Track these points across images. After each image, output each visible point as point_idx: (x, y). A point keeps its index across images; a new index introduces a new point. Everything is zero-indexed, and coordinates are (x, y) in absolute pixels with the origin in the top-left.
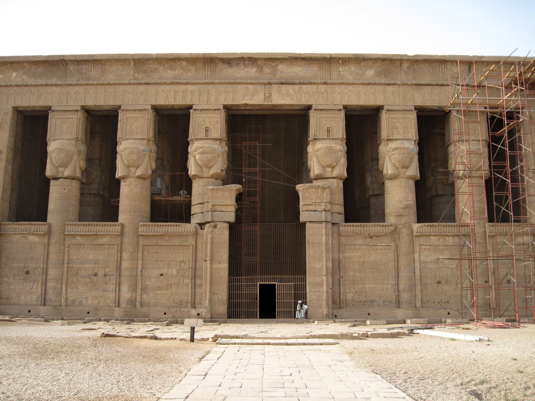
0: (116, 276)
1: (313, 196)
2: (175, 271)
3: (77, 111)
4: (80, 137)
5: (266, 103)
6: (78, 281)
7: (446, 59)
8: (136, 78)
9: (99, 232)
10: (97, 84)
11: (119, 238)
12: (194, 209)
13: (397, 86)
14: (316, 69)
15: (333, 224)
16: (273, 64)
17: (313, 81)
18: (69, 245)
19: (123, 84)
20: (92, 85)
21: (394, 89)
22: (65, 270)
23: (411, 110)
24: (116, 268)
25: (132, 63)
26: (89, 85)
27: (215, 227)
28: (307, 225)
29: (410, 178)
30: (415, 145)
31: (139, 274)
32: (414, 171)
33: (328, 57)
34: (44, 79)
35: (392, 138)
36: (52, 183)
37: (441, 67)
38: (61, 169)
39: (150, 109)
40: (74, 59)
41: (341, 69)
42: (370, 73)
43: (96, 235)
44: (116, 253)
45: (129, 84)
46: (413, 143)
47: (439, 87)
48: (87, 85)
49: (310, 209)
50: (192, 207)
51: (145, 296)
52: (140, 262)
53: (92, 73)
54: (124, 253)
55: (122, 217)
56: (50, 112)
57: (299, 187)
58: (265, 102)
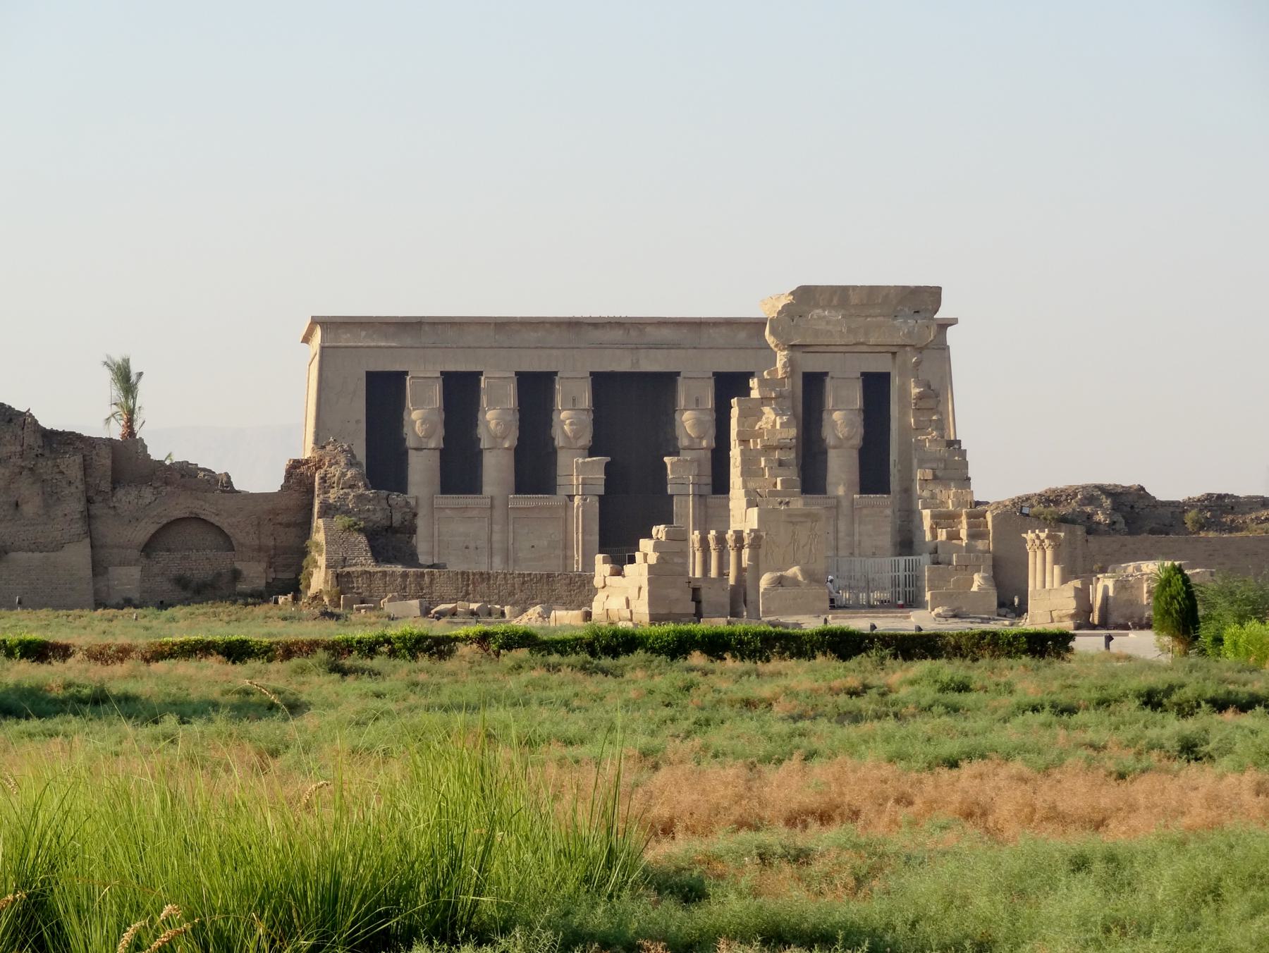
2: (546, 543)
3: (437, 378)
10: (457, 348)
11: (489, 511)
12: (560, 480)
14: (685, 331)
15: (700, 496)
16: (640, 326)
17: (682, 346)
22: (436, 544)
25: (493, 325)
27: (586, 500)
28: (675, 499)
31: (511, 547)
33: (698, 321)
36: (411, 453)
41: (711, 331)
42: (742, 335)
48: (446, 347)
50: (558, 478)
51: (516, 568)
52: (511, 535)
54: (494, 526)
57: (666, 459)
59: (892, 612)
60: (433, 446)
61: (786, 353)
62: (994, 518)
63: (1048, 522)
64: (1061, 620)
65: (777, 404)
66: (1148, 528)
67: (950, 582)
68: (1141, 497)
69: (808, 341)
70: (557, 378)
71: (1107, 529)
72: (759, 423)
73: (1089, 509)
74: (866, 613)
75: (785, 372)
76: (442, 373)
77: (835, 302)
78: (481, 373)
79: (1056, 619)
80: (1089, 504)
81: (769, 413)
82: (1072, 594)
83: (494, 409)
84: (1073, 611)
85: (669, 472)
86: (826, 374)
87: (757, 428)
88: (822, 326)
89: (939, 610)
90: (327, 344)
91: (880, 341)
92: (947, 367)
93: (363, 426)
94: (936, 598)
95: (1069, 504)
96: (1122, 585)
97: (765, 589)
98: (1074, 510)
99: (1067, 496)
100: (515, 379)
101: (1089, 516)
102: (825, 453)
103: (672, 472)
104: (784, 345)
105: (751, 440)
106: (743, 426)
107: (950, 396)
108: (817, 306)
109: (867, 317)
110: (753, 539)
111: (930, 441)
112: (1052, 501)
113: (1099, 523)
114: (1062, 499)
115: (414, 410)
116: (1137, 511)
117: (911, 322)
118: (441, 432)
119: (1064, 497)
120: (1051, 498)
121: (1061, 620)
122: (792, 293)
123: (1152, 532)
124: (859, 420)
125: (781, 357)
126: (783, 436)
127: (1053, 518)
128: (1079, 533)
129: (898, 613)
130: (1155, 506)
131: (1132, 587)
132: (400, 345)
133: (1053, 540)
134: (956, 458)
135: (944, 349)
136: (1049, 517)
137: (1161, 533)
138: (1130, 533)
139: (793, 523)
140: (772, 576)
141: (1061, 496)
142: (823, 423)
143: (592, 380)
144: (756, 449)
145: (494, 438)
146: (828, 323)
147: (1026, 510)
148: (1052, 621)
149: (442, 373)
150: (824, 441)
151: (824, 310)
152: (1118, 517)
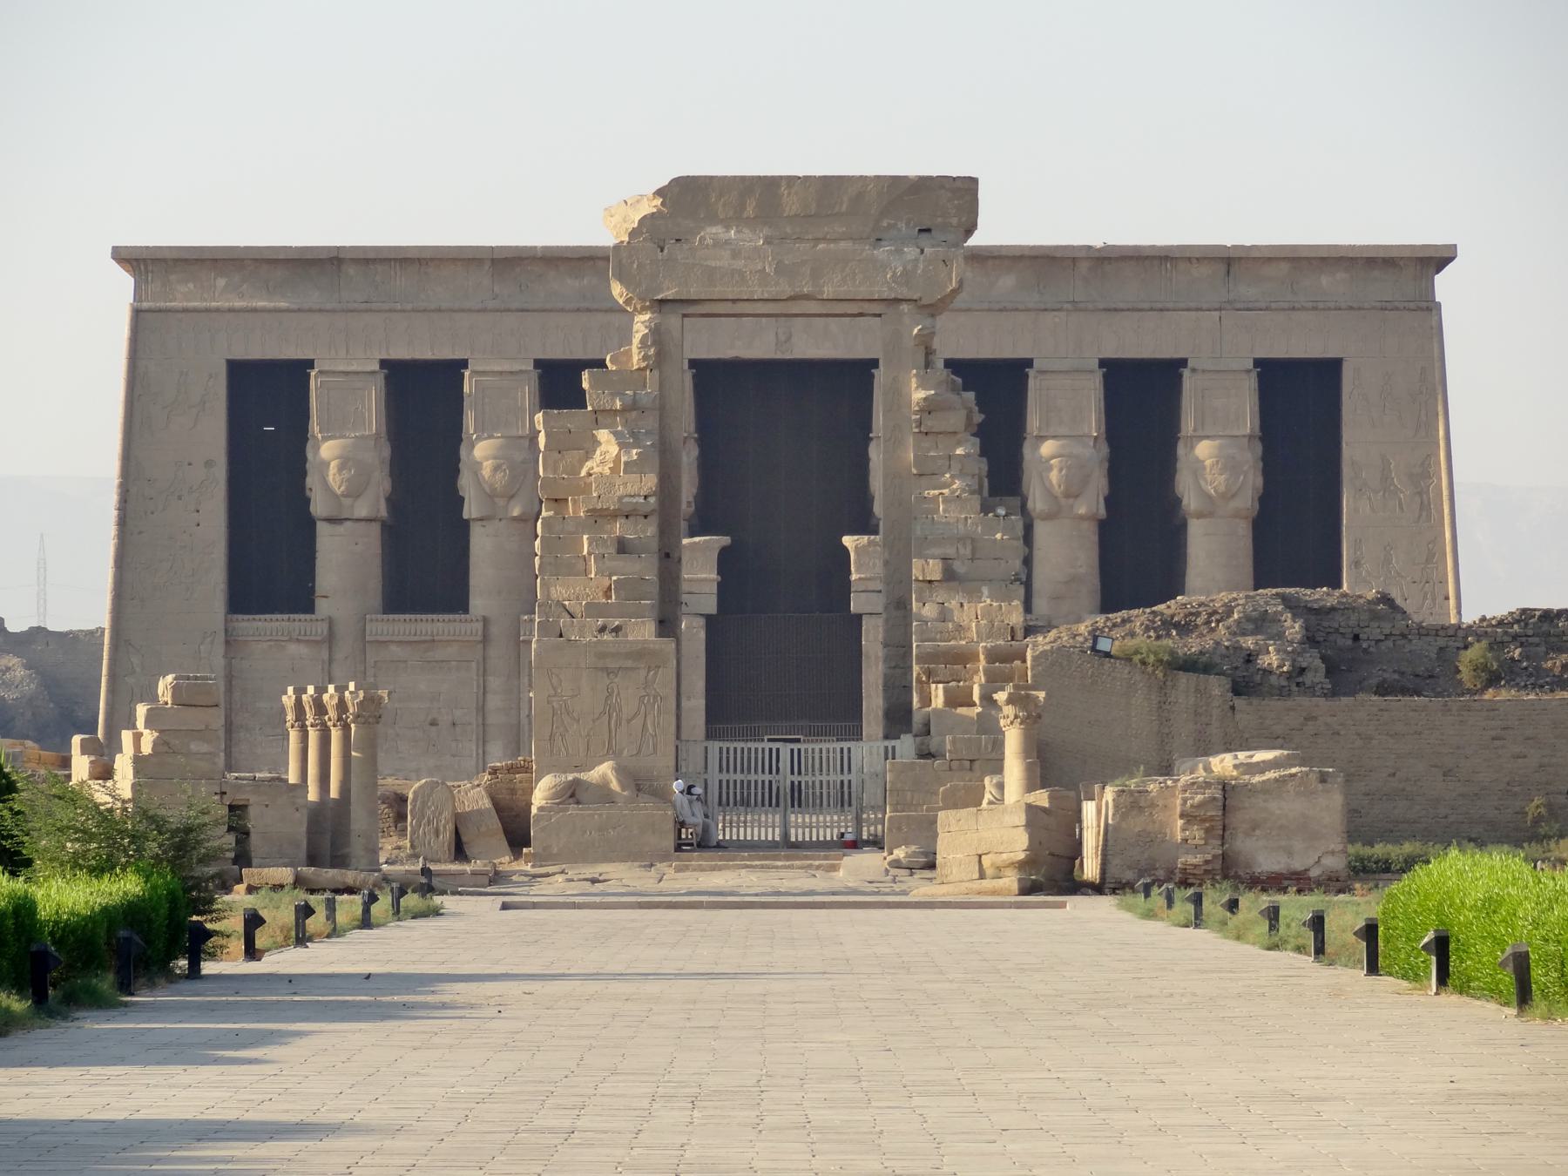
0: (478, 726)
1: (877, 561)
3: (373, 373)
4: (384, 428)
5: (779, 356)
6: (398, 735)
7: (1171, 255)
8: (497, 296)
9: (438, 635)
10: (414, 310)
13: (1065, 313)
18: (375, 662)
19: (470, 310)
20: (401, 311)
21: (1057, 320)
23: (1091, 372)
24: (477, 709)
26: (395, 311)
29: (1082, 518)
30: (1095, 446)
31: (524, 721)
32: (1091, 503)
34: (289, 295)
35: (1046, 434)
36: (322, 528)
37: (1163, 267)
38: (347, 502)
39: (531, 368)
40: (362, 257)
42: (1007, 282)
43: (434, 641)
44: (475, 678)
45: (484, 310)
46: (1092, 443)
47: (1156, 312)
48: (390, 311)
49: (870, 588)
53: (398, 283)
54: (490, 678)
55: (478, 603)
56: (313, 374)
57: (848, 541)
58: (778, 352)
59: (806, 858)
60: (362, 510)
61: (647, 317)
62: (1035, 659)
63: (1150, 669)
64: (999, 872)
65: (626, 423)
66: (1374, 681)
67: (936, 793)
68: (1376, 616)
69: (693, 292)
70: (1031, 373)
71: (1285, 683)
72: (589, 464)
73: (1249, 643)
74: (751, 858)
75: (645, 358)
76: (384, 363)
77: (750, 211)
78: (464, 364)
79: (989, 872)
80: (1253, 633)
81: (607, 443)
82: (1021, 819)
83: (490, 437)
84: (1021, 856)
85: (853, 569)
86: (1183, 362)
87: (583, 473)
88: (723, 260)
89: (900, 853)
90: (145, 305)
91: (844, 291)
92: (1436, 345)
93: (220, 472)
94: (899, 829)
95: (1212, 630)
96: (1131, 804)
97: (541, 809)
98: (1217, 643)
99: (1210, 615)
100: (534, 375)
101: (1250, 658)
102: (1183, 527)
103: (858, 571)
104: (643, 300)
105: (570, 498)
106: (555, 471)
107: (1440, 408)
108: (713, 219)
109: (817, 240)
110: (361, 704)
111: (946, 500)
112: (1177, 626)
113: (1267, 672)
114: (1199, 621)
115: (326, 439)
116: (1365, 645)
117: (911, 252)
118: (381, 484)
119: (1204, 616)
120: (1176, 619)
121: (999, 872)
122: (660, 193)
123: (1383, 690)
124: (1250, 459)
125: (641, 324)
126: (630, 490)
127: (1161, 661)
128: (1217, 692)
129: (818, 858)
130: (1404, 636)
131: (1153, 805)
132: (294, 306)
133: (1024, 708)
134: (998, 536)
135: (1429, 309)
136: (1152, 658)
137: (1404, 691)
138: (1334, 693)
139: (608, 671)
140: (558, 780)
141: (1198, 614)
142: (1179, 465)
143: (694, 376)
144: (577, 518)
145: (490, 496)
146: (736, 254)
147: (1104, 645)
148: (982, 876)
149: (384, 363)
150: (1179, 501)
151: (728, 228)
152: (1312, 659)
